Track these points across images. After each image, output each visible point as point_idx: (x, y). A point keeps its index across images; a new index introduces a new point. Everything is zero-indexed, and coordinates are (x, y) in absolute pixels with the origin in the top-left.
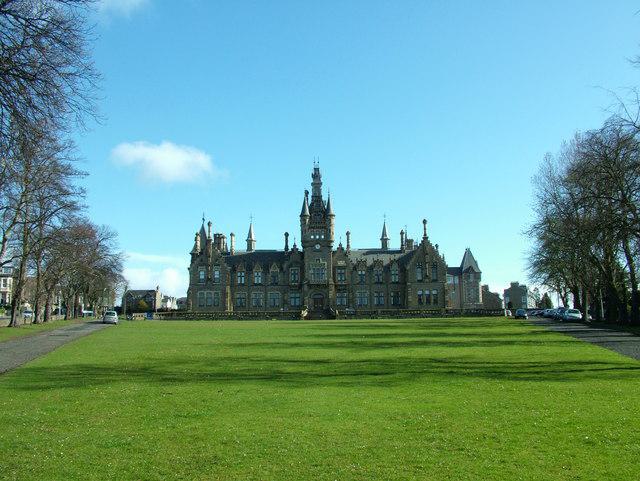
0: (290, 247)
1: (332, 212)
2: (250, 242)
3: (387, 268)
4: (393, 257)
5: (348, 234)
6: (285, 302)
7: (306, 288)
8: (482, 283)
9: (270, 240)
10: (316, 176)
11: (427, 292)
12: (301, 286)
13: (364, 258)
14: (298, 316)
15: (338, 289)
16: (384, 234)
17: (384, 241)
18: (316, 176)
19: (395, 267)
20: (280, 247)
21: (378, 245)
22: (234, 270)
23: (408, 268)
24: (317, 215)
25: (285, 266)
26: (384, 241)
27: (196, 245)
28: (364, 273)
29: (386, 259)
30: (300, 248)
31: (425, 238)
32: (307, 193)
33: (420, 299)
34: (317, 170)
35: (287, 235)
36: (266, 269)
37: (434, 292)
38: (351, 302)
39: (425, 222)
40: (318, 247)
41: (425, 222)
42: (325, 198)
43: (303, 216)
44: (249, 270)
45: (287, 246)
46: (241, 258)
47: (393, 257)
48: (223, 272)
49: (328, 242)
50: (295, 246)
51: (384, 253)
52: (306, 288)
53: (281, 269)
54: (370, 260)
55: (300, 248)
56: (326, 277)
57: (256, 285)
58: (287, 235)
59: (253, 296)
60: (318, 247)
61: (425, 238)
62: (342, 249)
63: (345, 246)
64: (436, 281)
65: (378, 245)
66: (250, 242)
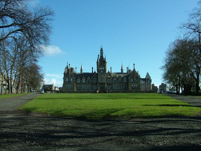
0: (94, 72)
1: (106, 61)
2: (81, 70)
3: (123, 78)
4: (124, 75)
5: (111, 68)
6: (92, 88)
7: (98, 84)
8: (152, 83)
9: (88, 70)
10: (102, 50)
11: (135, 86)
12: (97, 83)
13: (116, 75)
14: (96, 92)
15: (108, 84)
16: (122, 68)
17: (122, 70)
18: (102, 50)
19: (125, 79)
20: (91, 72)
21: (120, 72)
22: (77, 79)
23: (129, 78)
24: (102, 62)
26: (122, 70)
27: (65, 71)
29: (122, 76)
30: (97, 72)
31: (134, 69)
32: (99, 55)
33: (132, 88)
34: (102, 48)
35: (93, 68)
36: (86, 79)
37: (137, 86)
38: (112, 88)
39: (134, 64)
40: (102, 72)
41: (134, 64)
42: (104, 57)
43: (97, 62)
44: (81, 79)
45: (92, 72)
47: (124, 75)
48: (73, 79)
49: (105, 70)
50: (95, 71)
51: (122, 74)
52: (98, 84)
53: (91, 78)
54: (117, 76)
55: (97, 72)
56: (104, 81)
58: (93, 68)
59: (82, 86)
60: (102, 72)
61: (134, 69)
62: (109, 72)
63: (110, 72)
64: (137, 82)
65: (120, 72)
66: (81, 70)
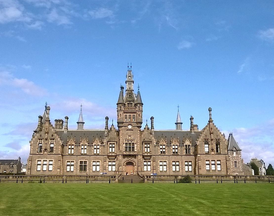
5: (152, 118)
24: (130, 104)
25: (105, 141)
35: (107, 118)
36: (90, 144)
40: (130, 127)
46: (72, 133)
52: (120, 158)
57: (82, 155)
60: (130, 127)
62: (148, 129)
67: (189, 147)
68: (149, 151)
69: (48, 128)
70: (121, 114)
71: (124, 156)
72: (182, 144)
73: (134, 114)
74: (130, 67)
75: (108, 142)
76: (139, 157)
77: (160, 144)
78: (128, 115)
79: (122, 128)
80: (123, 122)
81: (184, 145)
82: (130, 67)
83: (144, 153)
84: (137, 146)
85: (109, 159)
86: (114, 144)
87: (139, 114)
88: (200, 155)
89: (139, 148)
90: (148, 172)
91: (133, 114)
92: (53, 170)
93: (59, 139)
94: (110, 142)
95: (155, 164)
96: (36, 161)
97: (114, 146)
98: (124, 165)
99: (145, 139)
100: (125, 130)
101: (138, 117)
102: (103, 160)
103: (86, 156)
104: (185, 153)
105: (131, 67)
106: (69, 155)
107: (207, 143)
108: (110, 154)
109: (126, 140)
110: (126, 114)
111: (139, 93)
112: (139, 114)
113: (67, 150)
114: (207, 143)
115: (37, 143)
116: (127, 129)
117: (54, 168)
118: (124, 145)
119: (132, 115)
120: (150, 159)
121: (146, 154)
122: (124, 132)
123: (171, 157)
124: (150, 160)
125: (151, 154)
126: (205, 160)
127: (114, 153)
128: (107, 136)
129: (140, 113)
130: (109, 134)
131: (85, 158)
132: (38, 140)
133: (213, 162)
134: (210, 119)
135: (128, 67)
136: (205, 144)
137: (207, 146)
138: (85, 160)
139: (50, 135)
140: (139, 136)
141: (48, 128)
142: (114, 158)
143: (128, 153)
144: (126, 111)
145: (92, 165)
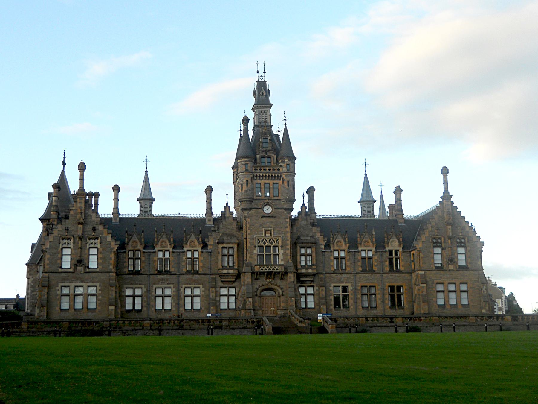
0: (217, 211)
9: (179, 202)
10: (262, 93)
18: (262, 93)
20: (197, 210)
25: (211, 242)
28: (343, 254)
31: (447, 196)
32: (246, 120)
35: (209, 190)
39: (445, 171)
40: (268, 210)
41: (445, 171)
50: (227, 207)
52: (247, 278)
60: (268, 210)
61: (447, 196)
67: (396, 254)
68: (310, 264)
69: (83, 212)
70: (247, 181)
71: (256, 275)
72: (380, 245)
73: (278, 181)
74: (261, 73)
75: (218, 243)
76: (290, 277)
77: (334, 247)
78: (263, 182)
79: (250, 213)
80: (254, 199)
81: (387, 249)
82: (261, 73)
83: (299, 267)
84: (285, 252)
85: (222, 281)
86: (233, 248)
87: (288, 182)
88: (423, 272)
89: (289, 257)
90: (309, 310)
91: (275, 181)
92: (99, 308)
93: (109, 238)
94: (223, 243)
95: (324, 293)
96: (57, 288)
97: (231, 252)
98: (256, 295)
99: (302, 238)
100: (257, 216)
101: (287, 187)
102: (207, 285)
103: (169, 277)
104: (387, 269)
105: (265, 72)
106: (131, 273)
107: (437, 245)
108: (225, 271)
109: (261, 241)
110: (259, 181)
111: (286, 130)
112: (288, 182)
113: (125, 262)
114: (439, 245)
115: (59, 247)
116: (262, 214)
117: (99, 302)
118: (256, 251)
119: (271, 182)
120: (312, 281)
121: (304, 271)
122: (255, 221)
123: (358, 276)
124: (312, 284)
125: (315, 271)
126: (435, 281)
127: (232, 268)
128: (215, 231)
129: (289, 178)
130: (221, 226)
131: (167, 280)
132: (61, 240)
133: (452, 287)
134: (446, 191)
135: (258, 72)
136: (434, 247)
137: (438, 250)
138: (168, 284)
139: (89, 228)
140: (288, 230)
141: (83, 212)
142: (234, 280)
143: (265, 269)
144: (258, 175)
145: (182, 296)
